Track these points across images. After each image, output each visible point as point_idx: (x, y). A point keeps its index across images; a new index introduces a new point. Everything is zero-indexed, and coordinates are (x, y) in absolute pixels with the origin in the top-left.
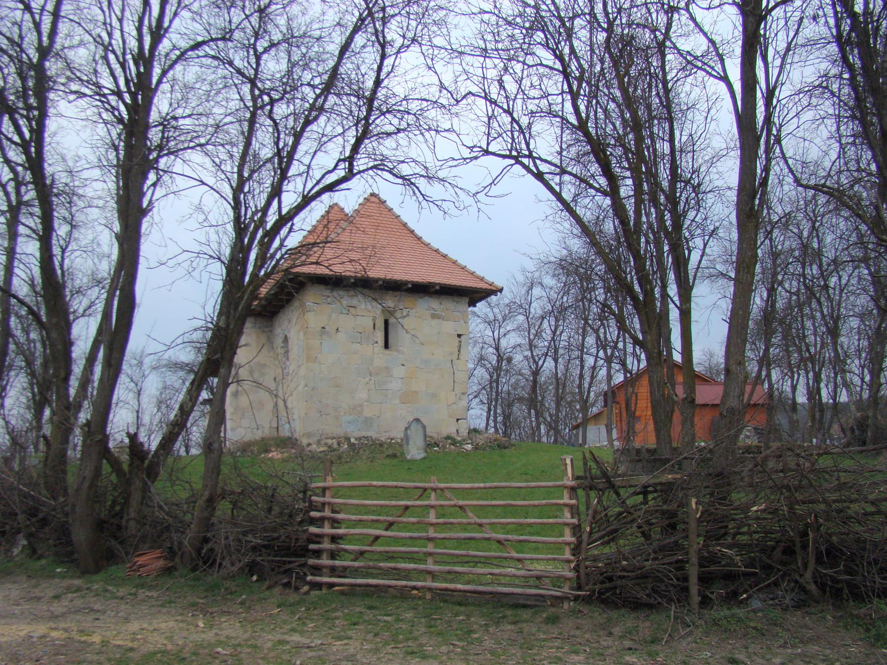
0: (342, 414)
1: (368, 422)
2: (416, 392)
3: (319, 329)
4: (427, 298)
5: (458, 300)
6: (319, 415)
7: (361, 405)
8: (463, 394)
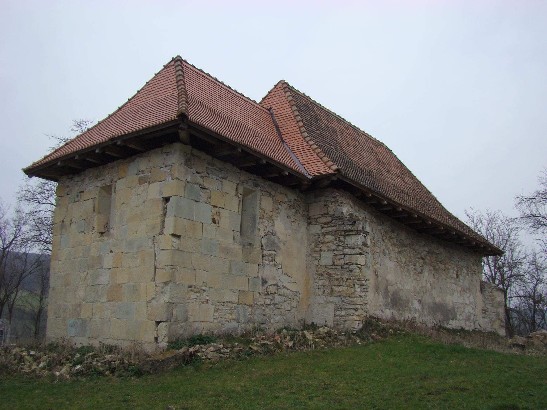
0: (68, 316)
1: (84, 323)
2: (120, 286)
4: (137, 159)
6: (55, 317)
7: (80, 305)
8: (166, 283)
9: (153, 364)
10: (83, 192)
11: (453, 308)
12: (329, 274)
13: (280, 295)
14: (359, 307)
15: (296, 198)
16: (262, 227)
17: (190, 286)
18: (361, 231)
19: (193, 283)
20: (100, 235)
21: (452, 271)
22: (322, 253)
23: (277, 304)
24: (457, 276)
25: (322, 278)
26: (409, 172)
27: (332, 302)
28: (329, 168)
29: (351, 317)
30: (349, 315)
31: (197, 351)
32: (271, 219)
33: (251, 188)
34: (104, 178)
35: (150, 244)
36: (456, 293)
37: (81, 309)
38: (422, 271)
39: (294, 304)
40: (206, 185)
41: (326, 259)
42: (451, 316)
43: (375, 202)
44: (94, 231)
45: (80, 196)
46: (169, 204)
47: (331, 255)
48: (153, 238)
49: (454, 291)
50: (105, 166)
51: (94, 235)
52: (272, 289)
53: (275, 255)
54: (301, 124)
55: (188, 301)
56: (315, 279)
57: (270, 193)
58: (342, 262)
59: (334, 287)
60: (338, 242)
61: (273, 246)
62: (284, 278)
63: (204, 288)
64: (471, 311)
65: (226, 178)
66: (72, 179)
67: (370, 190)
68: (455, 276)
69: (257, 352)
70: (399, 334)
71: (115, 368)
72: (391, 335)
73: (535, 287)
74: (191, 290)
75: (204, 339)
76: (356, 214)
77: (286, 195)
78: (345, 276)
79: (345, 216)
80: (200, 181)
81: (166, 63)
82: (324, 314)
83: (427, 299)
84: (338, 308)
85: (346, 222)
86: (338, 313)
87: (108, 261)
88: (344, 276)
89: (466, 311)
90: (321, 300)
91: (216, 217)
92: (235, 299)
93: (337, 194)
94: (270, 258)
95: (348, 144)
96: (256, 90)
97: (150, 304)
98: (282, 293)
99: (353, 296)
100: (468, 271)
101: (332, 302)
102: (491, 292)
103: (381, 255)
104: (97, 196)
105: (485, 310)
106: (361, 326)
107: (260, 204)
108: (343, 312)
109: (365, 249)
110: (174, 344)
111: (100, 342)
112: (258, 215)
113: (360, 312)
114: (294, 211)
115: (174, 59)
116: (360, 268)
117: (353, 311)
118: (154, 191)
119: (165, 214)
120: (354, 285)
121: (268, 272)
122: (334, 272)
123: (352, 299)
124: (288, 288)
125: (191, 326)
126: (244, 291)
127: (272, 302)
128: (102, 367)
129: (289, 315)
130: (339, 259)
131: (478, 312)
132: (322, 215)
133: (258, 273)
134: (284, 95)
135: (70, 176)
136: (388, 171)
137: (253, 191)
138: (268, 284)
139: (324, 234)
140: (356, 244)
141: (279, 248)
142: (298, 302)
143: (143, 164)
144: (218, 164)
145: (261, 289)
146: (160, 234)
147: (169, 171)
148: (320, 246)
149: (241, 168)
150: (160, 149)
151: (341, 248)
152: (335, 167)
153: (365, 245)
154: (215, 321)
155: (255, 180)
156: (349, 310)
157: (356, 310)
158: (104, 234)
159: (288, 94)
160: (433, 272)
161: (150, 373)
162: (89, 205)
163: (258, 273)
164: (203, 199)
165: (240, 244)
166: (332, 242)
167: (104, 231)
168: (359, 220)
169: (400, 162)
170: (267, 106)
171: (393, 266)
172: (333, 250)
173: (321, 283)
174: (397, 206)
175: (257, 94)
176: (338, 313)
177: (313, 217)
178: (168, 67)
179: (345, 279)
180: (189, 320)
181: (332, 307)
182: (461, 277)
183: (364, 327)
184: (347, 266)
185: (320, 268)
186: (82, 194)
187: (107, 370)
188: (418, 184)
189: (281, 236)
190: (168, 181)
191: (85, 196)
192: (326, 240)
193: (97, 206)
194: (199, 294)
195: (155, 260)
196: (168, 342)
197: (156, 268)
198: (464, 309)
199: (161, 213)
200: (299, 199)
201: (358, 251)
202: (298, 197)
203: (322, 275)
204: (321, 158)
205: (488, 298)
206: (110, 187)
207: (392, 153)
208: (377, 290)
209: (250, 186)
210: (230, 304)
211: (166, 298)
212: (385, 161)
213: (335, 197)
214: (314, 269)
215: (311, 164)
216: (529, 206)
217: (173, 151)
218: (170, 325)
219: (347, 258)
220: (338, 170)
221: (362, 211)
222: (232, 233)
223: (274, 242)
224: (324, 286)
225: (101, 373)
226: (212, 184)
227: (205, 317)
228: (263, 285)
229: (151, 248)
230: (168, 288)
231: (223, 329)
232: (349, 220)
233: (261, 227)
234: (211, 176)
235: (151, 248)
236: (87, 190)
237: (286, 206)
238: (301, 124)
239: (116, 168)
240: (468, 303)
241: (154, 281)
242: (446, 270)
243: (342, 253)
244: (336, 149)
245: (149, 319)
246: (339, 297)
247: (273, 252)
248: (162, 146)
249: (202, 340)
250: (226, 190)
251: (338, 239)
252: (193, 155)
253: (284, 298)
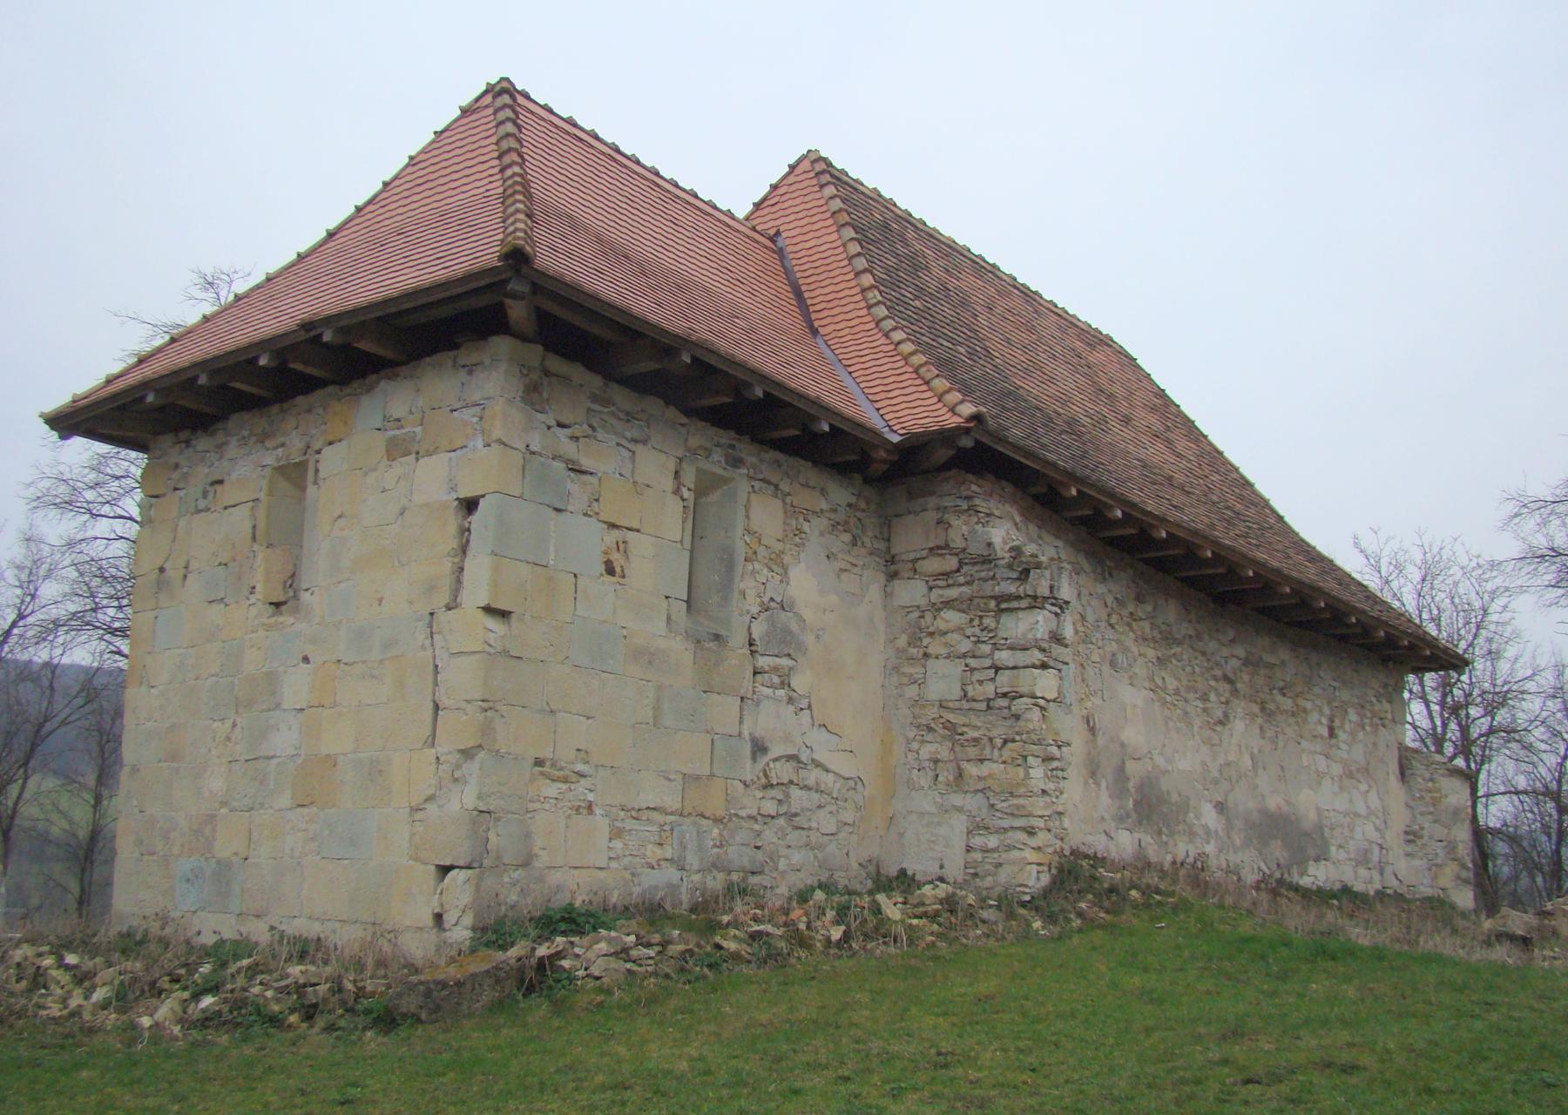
0: (176, 850)
2: (331, 761)
3: (155, 575)
4: (383, 384)
5: (474, 357)
6: (137, 855)
7: (212, 818)
8: (467, 754)
9: (428, 994)
10: (220, 482)
11: (1320, 828)
12: (950, 727)
13: (807, 788)
14: (1040, 823)
15: (853, 500)
16: (751, 587)
17: (539, 762)
18: (1045, 598)
19: (547, 753)
20: (271, 609)
21: (1314, 717)
22: (931, 663)
23: (796, 815)
24: (1331, 730)
25: (929, 737)
26: (1189, 424)
27: (959, 809)
28: (952, 410)
29: (1015, 854)
30: (1010, 848)
31: (559, 955)
32: (777, 563)
33: (721, 472)
34: (282, 439)
35: (422, 636)
36: (1327, 784)
37: (214, 831)
38: (1226, 715)
39: (848, 816)
40: (586, 463)
41: (943, 680)
42: (1311, 852)
43: (1087, 512)
44: (253, 599)
45: (211, 495)
46: (476, 518)
47: (956, 669)
48: (428, 618)
49: (1320, 776)
50: (286, 406)
51: (254, 611)
52: (783, 771)
53: (791, 669)
54: (867, 280)
55: (531, 806)
56: (908, 742)
57: (776, 486)
58: (989, 689)
59: (964, 765)
60: (977, 630)
61: (787, 642)
62: (817, 737)
63: (580, 767)
64: (1374, 835)
65: (645, 442)
66: (188, 443)
67: (1072, 477)
68: (1325, 733)
69: (736, 957)
70: (1159, 903)
71: (315, 1006)
72: (1135, 906)
73: (1561, 765)
74: (542, 774)
75: (581, 920)
76: (1030, 549)
77: (823, 492)
78: (999, 732)
79: (1000, 554)
80: (569, 449)
81: (466, 101)
82: (936, 843)
83: (1242, 800)
84: (979, 828)
85: (1002, 572)
86: (977, 841)
87: (297, 687)
88: (994, 733)
89: (1358, 836)
90: (926, 801)
91: (617, 559)
92: (672, 801)
93: (974, 488)
94: (776, 680)
95: (1008, 341)
96: (734, 181)
97: (419, 815)
98: (811, 782)
99: (1022, 790)
100: (1362, 716)
101: (959, 809)
102: (1431, 780)
103: (1106, 669)
104: (262, 496)
105: (1414, 833)
106: (1045, 879)
107: (748, 517)
108: (991, 838)
109: (1057, 650)
110: (493, 933)
111: (272, 928)
112: (741, 551)
113: (1042, 838)
114: (847, 537)
115: (490, 89)
116: (1042, 709)
117: (1023, 836)
118: (433, 480)
119: (464, 549)
120: (1025, 758)
121: (772, 719)
122: (966, 721)
123: (1020, 801)
124: (831, 767)
125: (541, 880)
126: (698, 778)
127: (783, 809)
128: (278, 1001)
129: (832, 847)
130: (981, 682)
131: (1393, 837)
132: (931, 549)
133: (741, 722)
134: (818, 195)
135: (184, 435)
136: (1127, 421)
137: (725, 481)
138: (771, 755)
139: (936, 608)
140: (1030, 636)
141: (802, 648)
142: (858, 809)
143: (398, 400)
144: (623, 398)
145: (749, 770)
146: (449, 608)
147: (475, 420)
148: (926, 641)
149: (689, 412)
150: (451, 354)
151: (986, 648)
152: (968, 409)
153: (1057, 638)
154: (614, 865)
155: (732, 447)
156: (1010, 834)
157: (1031, 832)
158: (284, 608)
159: (830, 191)
160: (1259, 721)
161: (419, 1021)
162: (240, 520)
163: (741, 722)
164: (578, 502)
165: (688, 635)
166: (960, 629)
167: (282, 599)
168: (1038, 566)
169: (1161, 394)
170: (769, 226)
171: (1140, 702)
172: (964, 656)
173: (926, 751)
174: (1152, 526)
175: (737, 193)
176: (977, 841)
177: (904, 557)
178: (474, 112)
179: (999, 742)
180: (536, 864)
181: (960, 823)
182: (1342, 736)
183: (1053, 882)
184: (1003, 702)
185: (923, 707)
186: (218, 487)
187: (292, 1011)
188: (1214, 458)
189: (807, 614)
190: (475, 449)
191: (228, 494)
192: (942, 625)
193: (262, 525)
194: (564, 786)
195: (436, 684)
196: (474, 929)
197: (437, 707)
198: (1352, 831)
199: (454, 543)
200: (863, 505)
201: (1037, 656)
202: (859, 496)
203: (930, 729)
204: (927, 383)
205: (1422, 798)
206: (302, 466)
207: (1139, 367)
208: (1093, 774)
209: (715, 464)
210: (656, 816)
211: (467, 797)
212: (1117, 389)
213: (968, 498)
214: (906, 711)
215: (897, 400)
216: (1544, 523)
217: (487, 361)
218: (480, 878)
219: (1004, 678)
220: (977, 418)
221: (1048, 538)
222: (664, 603)
223: (787, 631)
224: (936, 761)
225: (274, 1021)
226: (604, 457)
227: (582, 855)
228: (754, 759)
229: (423, 647)
230: (472, 768)
231: (638, 889)
232: (1010, 567)
233: (749, 585)
234: (600, 435)
235: (423, 647)
236: (234, 476)
237: (822, 523)
238: (867, 280)
239: (321, 411)
240: (1363, 812)
241: (433, 745)
242: (1298, 713)
243: (988, 662)
244: (971, 354)
245: (415, 860)
246: (980, 795)
247: (785, 662)
248: (456, 346)
249: (572, 921)
250: (643, 477)
251: (976, 622)
252: (547, 373)
253: (816, 796)
